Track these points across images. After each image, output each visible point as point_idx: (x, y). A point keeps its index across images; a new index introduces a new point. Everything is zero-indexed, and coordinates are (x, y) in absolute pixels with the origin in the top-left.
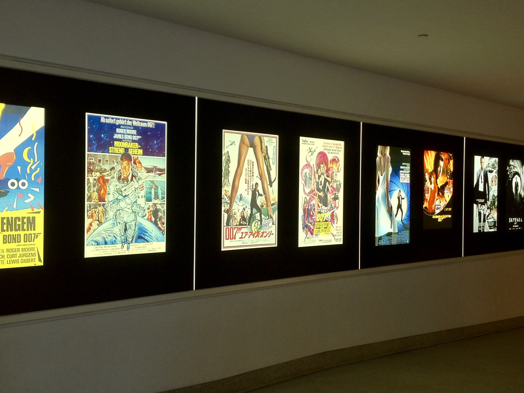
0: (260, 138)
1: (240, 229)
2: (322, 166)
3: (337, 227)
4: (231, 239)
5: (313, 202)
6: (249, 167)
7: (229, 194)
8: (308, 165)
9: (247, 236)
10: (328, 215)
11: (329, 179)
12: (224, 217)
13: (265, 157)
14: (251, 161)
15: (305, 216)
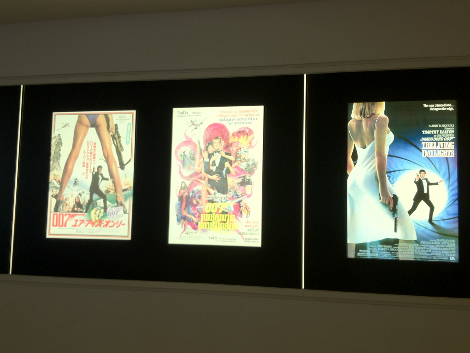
0: (106, 116)
1: (73, 216)
2: (216, 141)
3: (248, 222)
4: (59, 226)
5: (198, 188)
6: (90, 148)
7: (60, 178)
8: (188, 142)
9: (83, 225)
10: (230, 205)
11: (232, 158)
12: (52, 202)
13: (113, 137)
14: (91, 142)
15: (181, 204)
